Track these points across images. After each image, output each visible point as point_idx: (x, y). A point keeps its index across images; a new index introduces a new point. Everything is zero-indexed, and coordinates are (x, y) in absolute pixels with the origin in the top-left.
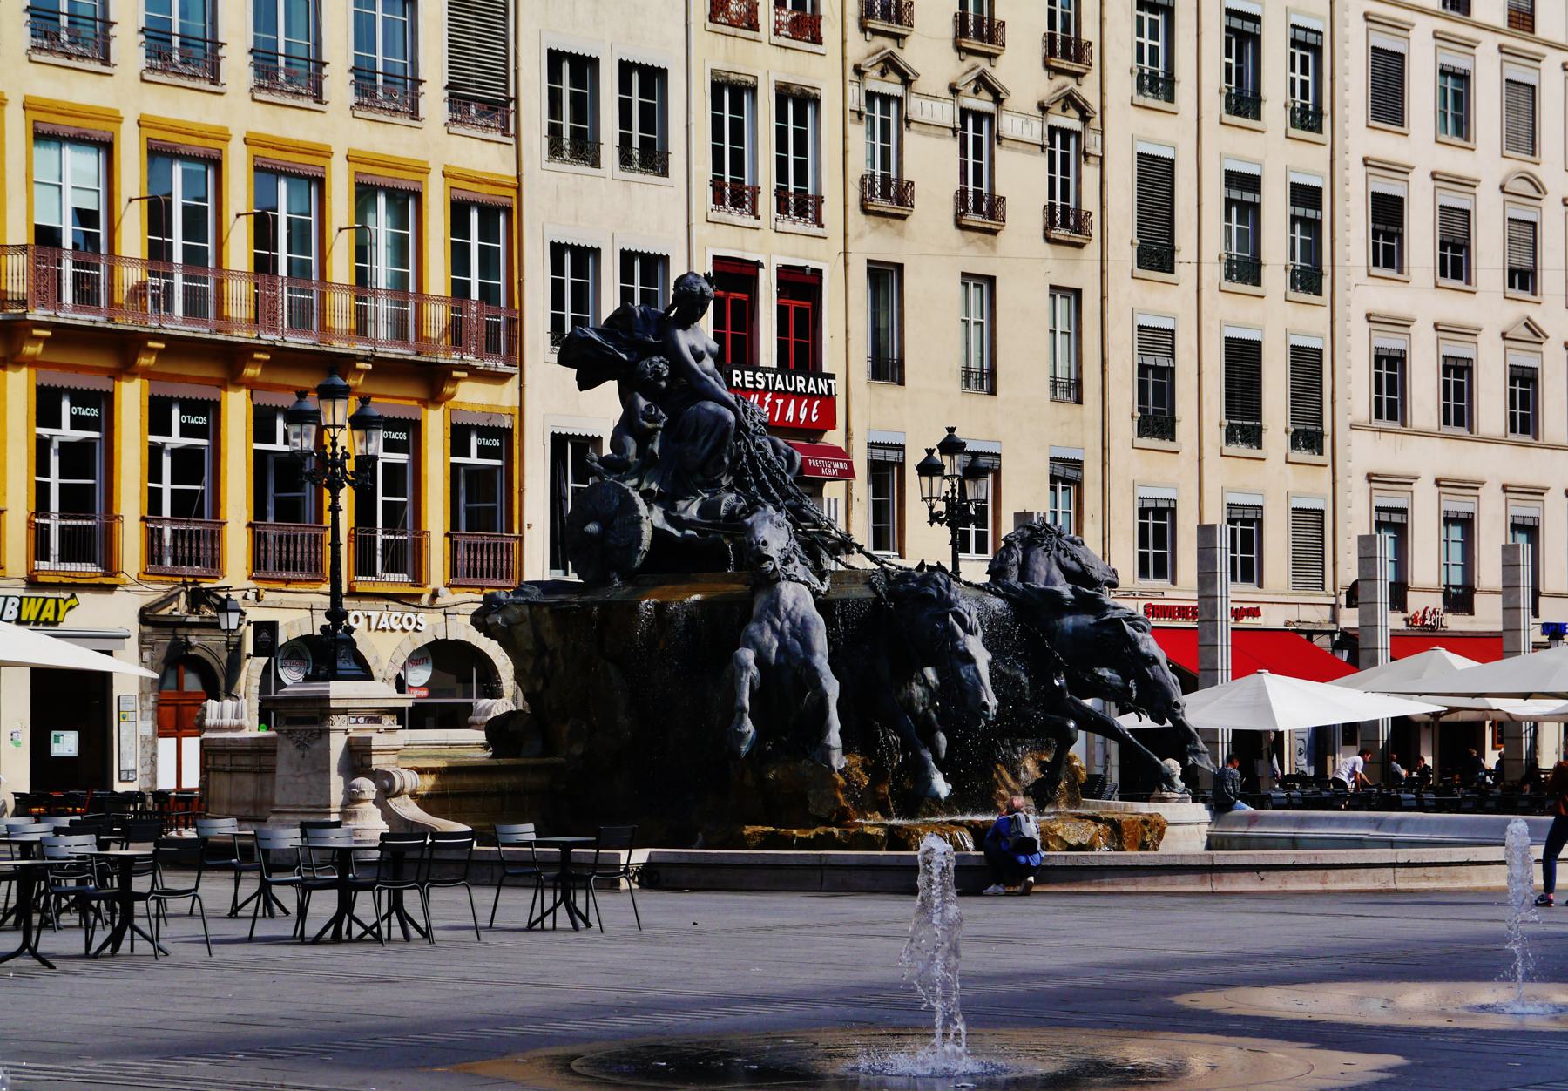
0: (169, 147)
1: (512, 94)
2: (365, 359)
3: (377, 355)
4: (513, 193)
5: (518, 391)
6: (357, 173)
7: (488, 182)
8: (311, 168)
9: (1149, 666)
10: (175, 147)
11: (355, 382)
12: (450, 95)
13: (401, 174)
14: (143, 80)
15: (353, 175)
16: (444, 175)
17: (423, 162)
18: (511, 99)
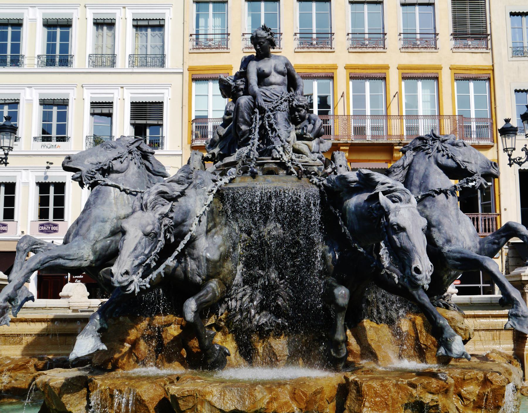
0: (308, 75)
1: (489, 32)
2: (399, 144)
3: (402, 142)
4: (491, 72)
5: (496, 153)
6: (402, 73)
7: (475, 69)
8: (378, 74)
9: (396, 233)
10: (311, 74)
11: (398, 155)
12: (454, 38)
13: (426, 71)
14: (295, 52)
15: (401, 75)
16: (450, 69)
17: (438, 65)
18: (489, 35)
